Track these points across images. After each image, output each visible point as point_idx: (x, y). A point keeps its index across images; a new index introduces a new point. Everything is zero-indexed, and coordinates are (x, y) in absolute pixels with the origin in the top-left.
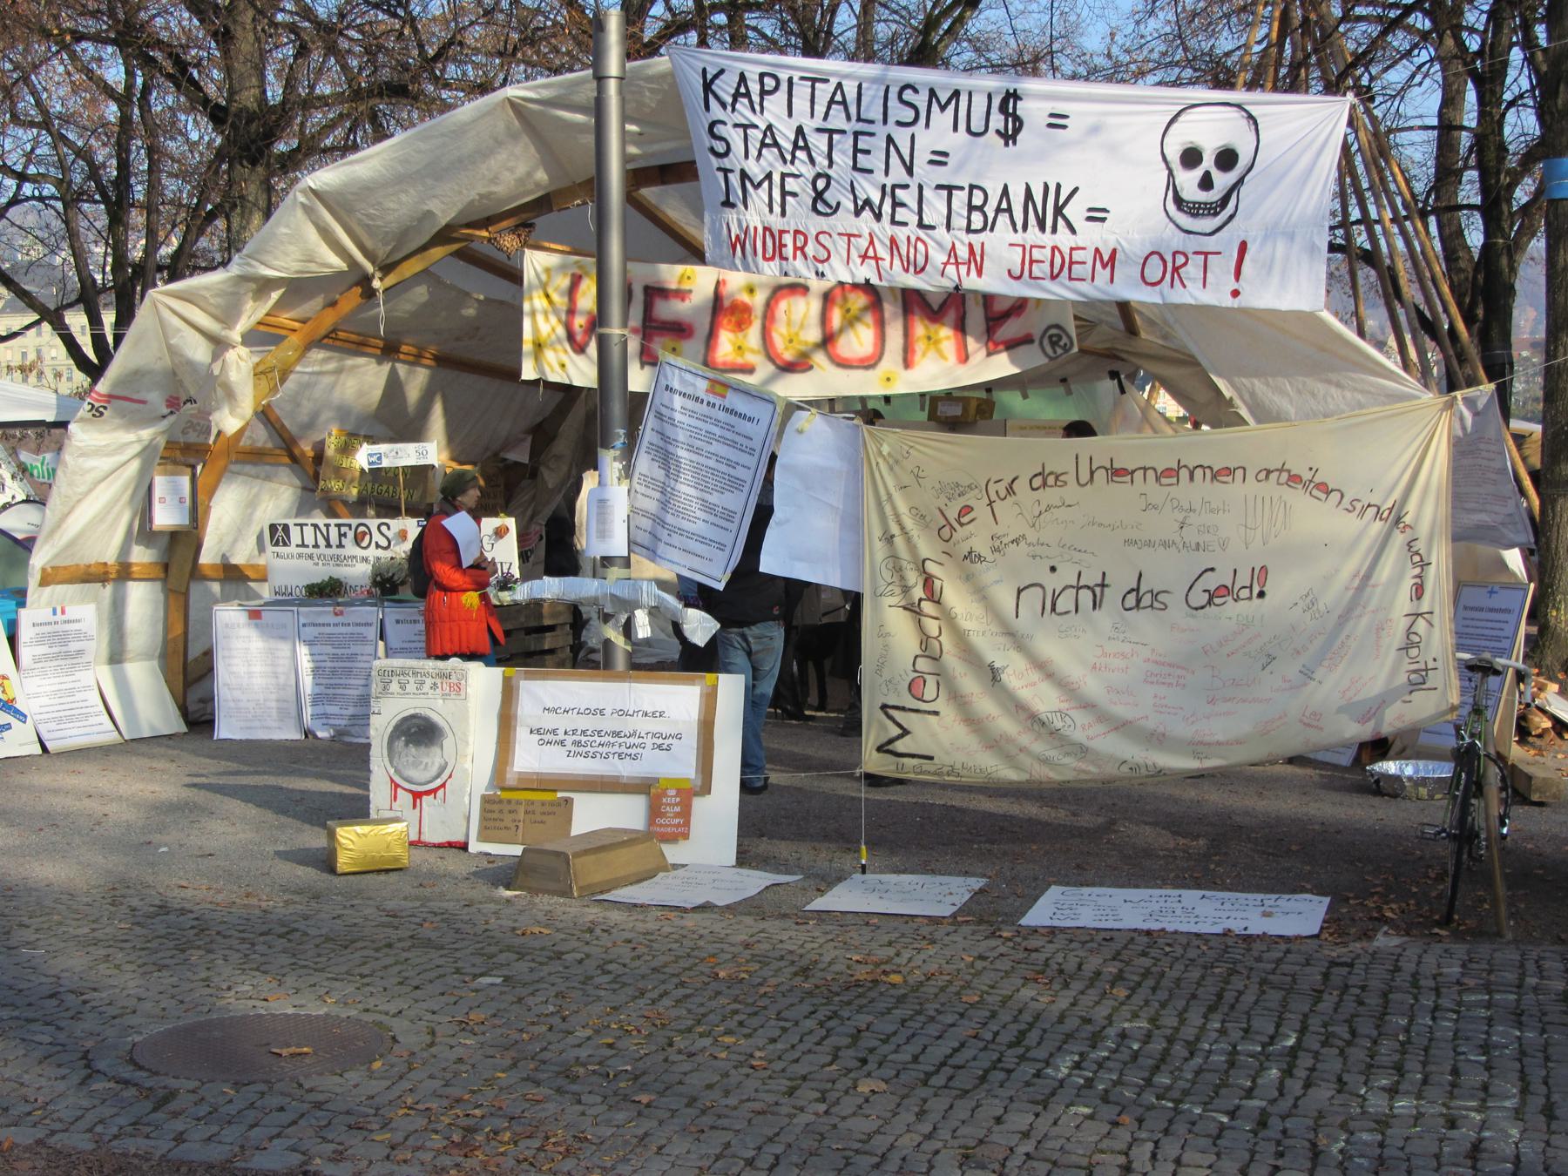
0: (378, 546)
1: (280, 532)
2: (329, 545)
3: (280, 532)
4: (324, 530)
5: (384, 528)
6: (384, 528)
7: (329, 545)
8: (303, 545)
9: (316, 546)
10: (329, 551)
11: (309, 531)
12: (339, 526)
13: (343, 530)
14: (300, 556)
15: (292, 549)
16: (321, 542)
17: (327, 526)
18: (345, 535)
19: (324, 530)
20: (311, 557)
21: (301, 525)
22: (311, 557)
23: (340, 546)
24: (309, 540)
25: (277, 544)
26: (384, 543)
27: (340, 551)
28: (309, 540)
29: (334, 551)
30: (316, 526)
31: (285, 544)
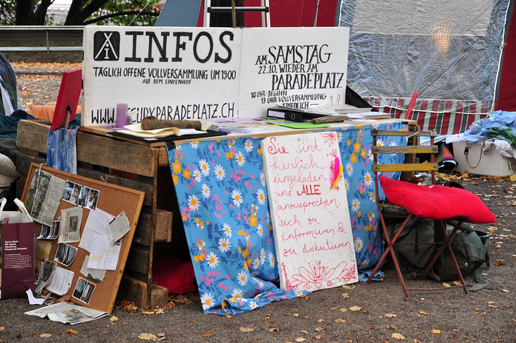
0: (218, 59)
1: (108, 42)
2: (164, 59)
3: (108, 42)
4: (161, 39)
5: (226, 38)
6: (226, 38)
7: (164, 59)
8: (134, 59)
9: (150, 59)
10: (164, 66)
11: (143, 41)
12: (178, 35)
13: (183, 39)
14: (129, 72)
15: (121, 64)
16: (156, 54)
17: (165, 35)
18: (183, 46)
19: (161, 39)
20: (141, 73)
21: (135, 34)
22: (141, 73)
23: (177, 59)
24: (142, 53)
25: (101, 58)
26: (224, 55)
27: (177, 65)
28: (142, 53)
29: (170, 65)
30: (152, 35)
31: (112, 58)
